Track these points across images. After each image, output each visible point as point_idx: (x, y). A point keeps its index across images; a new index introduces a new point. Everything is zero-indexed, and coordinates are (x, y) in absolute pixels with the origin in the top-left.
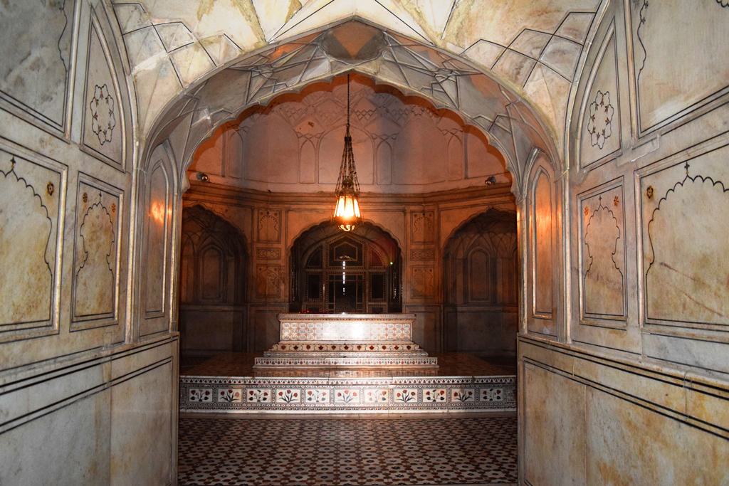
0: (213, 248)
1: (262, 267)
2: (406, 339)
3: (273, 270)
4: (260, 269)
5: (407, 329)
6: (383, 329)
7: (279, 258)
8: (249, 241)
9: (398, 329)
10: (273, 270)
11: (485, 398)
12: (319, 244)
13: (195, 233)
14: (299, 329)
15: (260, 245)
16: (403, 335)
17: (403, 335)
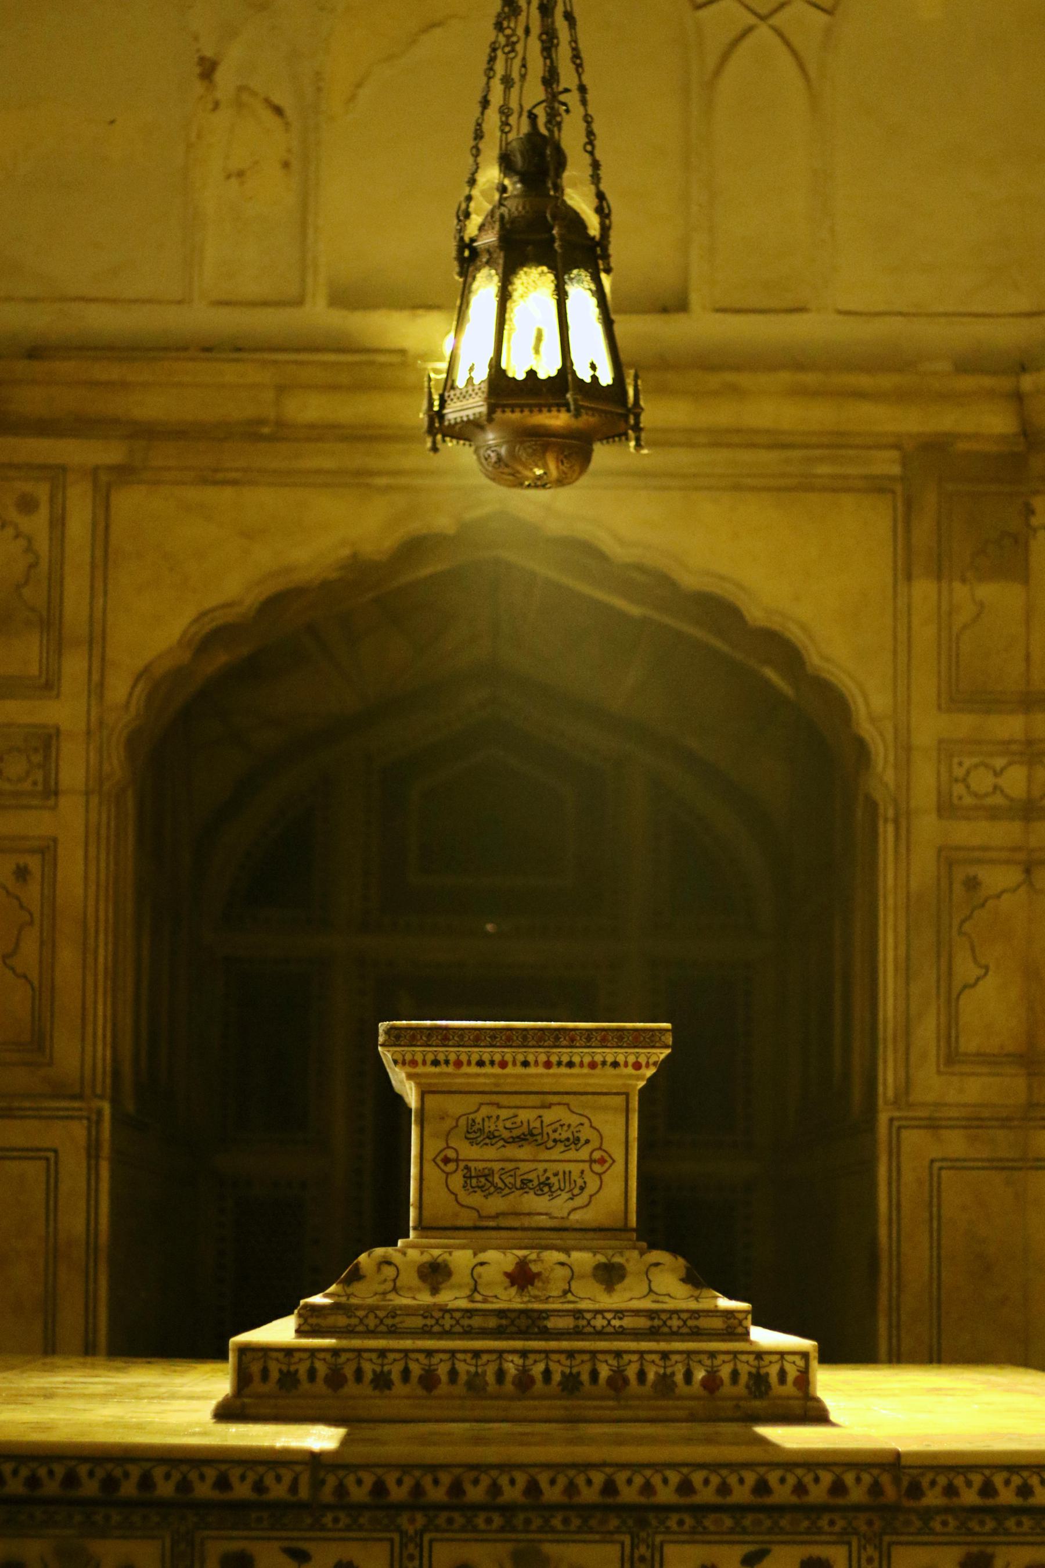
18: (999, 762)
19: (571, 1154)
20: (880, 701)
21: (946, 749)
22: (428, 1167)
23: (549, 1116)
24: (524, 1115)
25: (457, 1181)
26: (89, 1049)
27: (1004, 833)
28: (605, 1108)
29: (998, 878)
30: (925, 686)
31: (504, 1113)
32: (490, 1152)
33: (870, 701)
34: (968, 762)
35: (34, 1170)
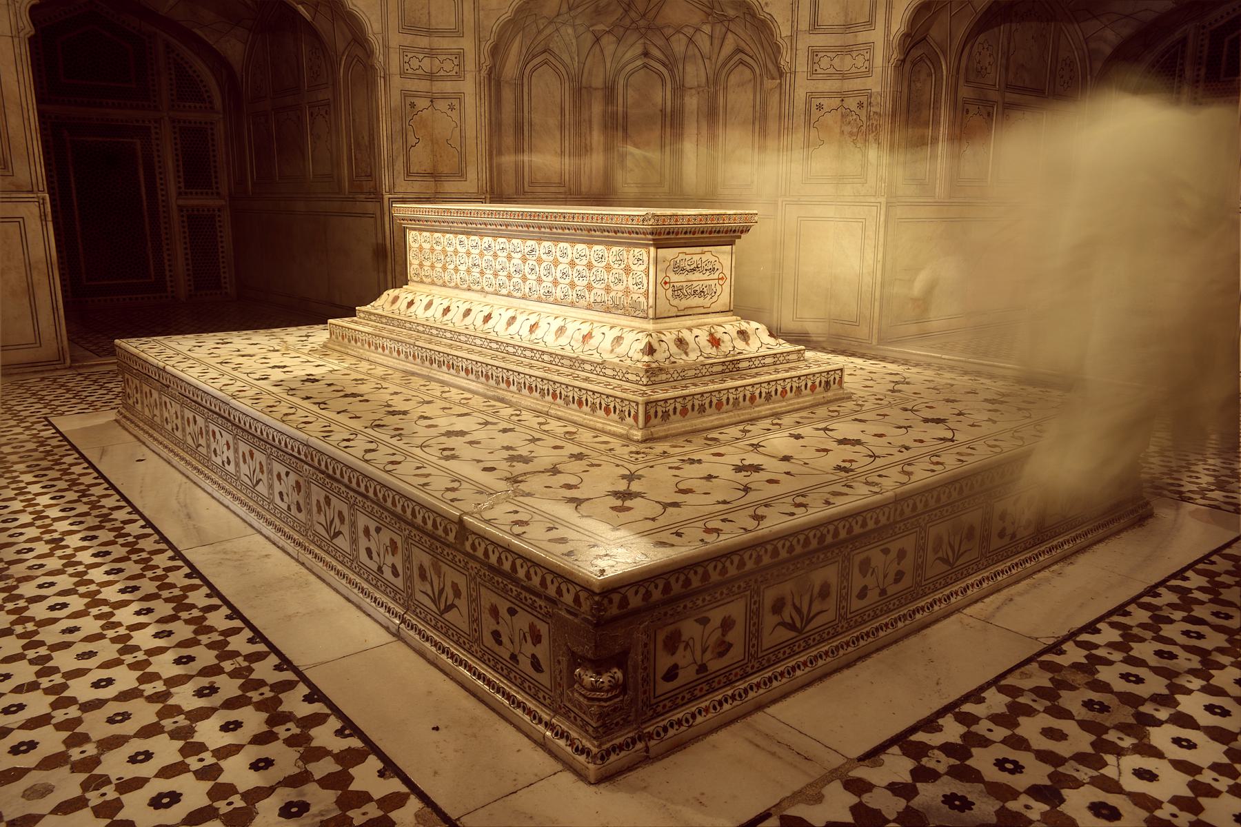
0: (742, 62)
1: (824, 102)
2: (635, 306)
3: (854, 107)
4: (820, 107)
5: (639, 269)
6: (581, 264)
7: (869, 72)
8: (785, 30)
9: (618, 269)
10: (854, 107)
11: (496, 635)
12: (1177, 35)
13: (698, 30)
14: (432, 250)
15: (819, 40)
16: (627, 292)
17: (627, 292)
18: (421, 56)
19: (712, 277)
20: (377, 27)
21: (403, 49)
22: (659, 286)
23: (704, 258)
24: (696, 258)
25: (670, 292)
26: (33, 168)
27: (423, 86)
28: (724, 253)
29: (422, 103)
30: (393, 22)
31: (688, 257)
32: (682, 278)
33: (373, 25)
34: (410, 55)
35: (13, 228)
